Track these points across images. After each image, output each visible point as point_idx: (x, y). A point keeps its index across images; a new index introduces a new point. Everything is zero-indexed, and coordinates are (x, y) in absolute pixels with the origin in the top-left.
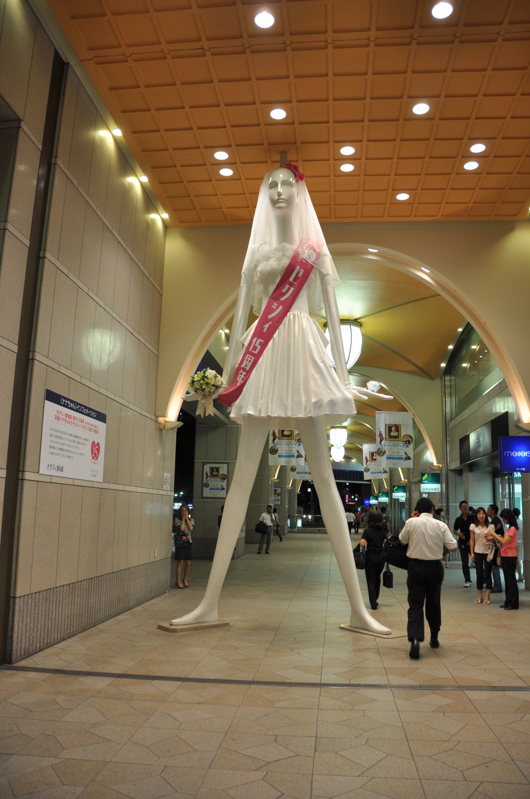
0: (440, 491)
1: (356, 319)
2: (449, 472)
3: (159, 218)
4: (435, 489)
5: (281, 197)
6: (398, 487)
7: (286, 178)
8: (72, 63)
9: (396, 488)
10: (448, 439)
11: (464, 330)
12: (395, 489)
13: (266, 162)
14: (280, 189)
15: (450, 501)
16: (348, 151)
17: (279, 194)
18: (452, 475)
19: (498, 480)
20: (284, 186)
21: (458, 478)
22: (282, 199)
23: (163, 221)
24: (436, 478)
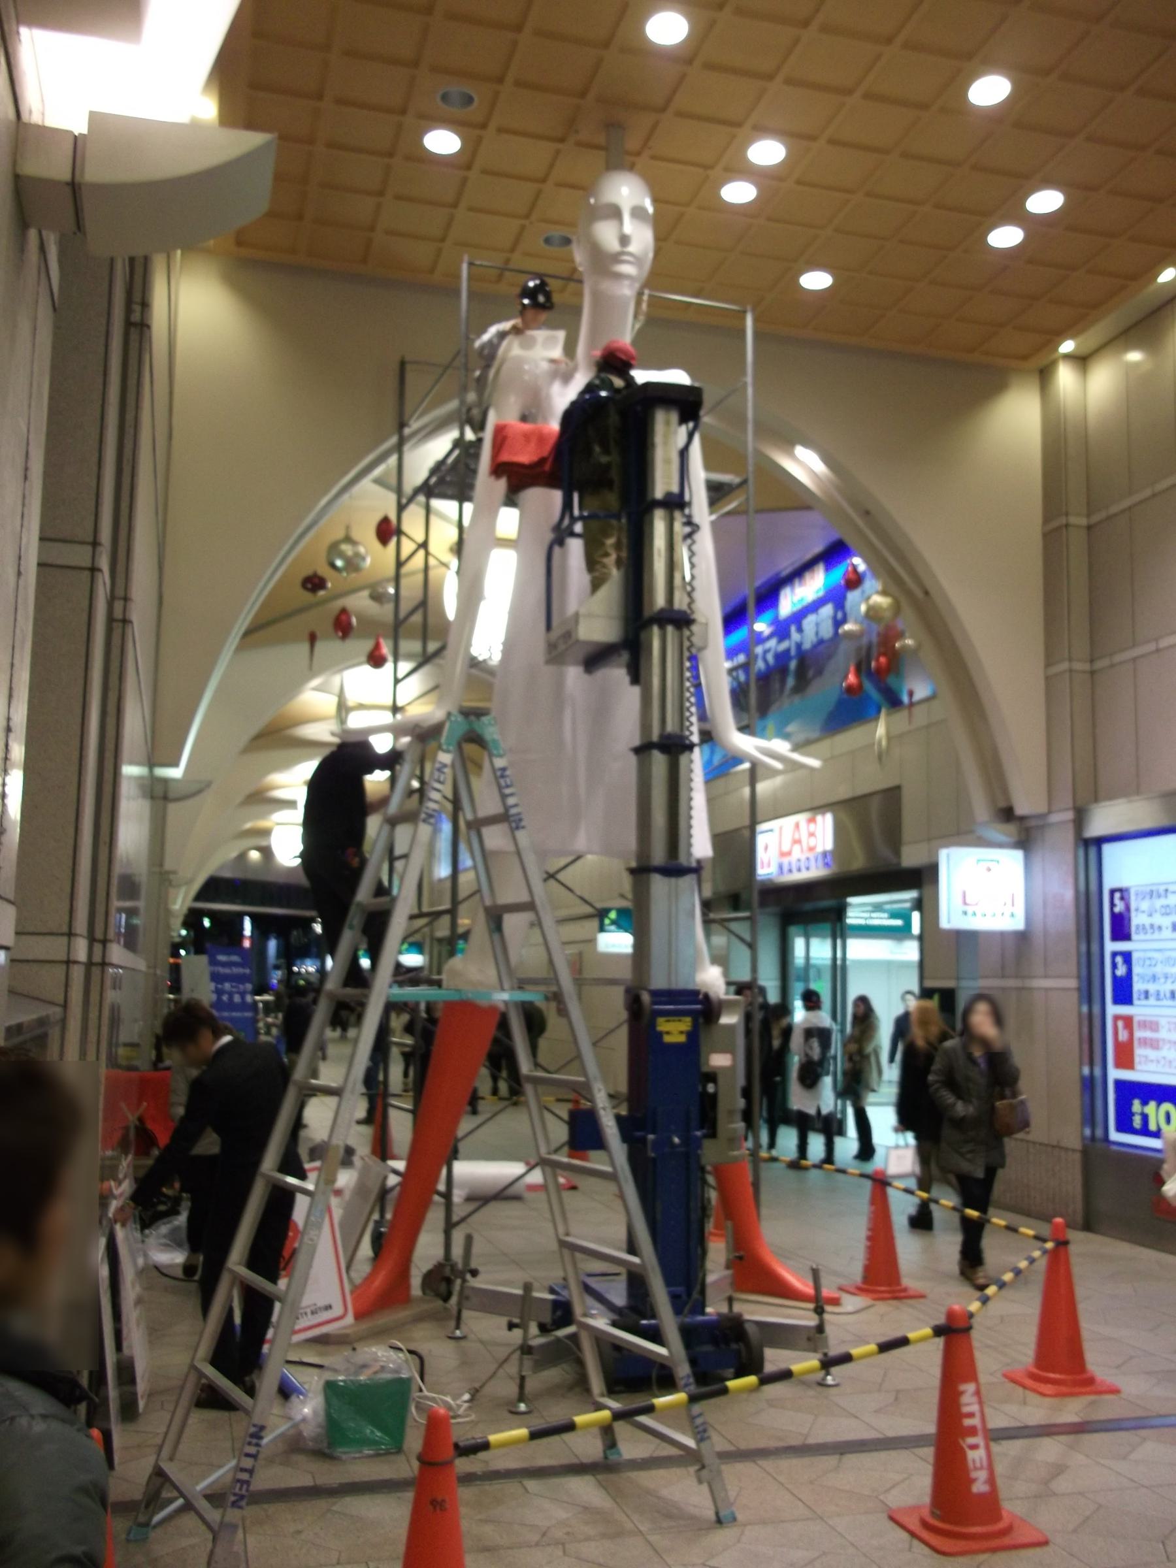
5: (632, 248)
7: (635, 201)
13: (562, 140)
16: (767, 152)
17: (624, 240)
19: (792, 930)
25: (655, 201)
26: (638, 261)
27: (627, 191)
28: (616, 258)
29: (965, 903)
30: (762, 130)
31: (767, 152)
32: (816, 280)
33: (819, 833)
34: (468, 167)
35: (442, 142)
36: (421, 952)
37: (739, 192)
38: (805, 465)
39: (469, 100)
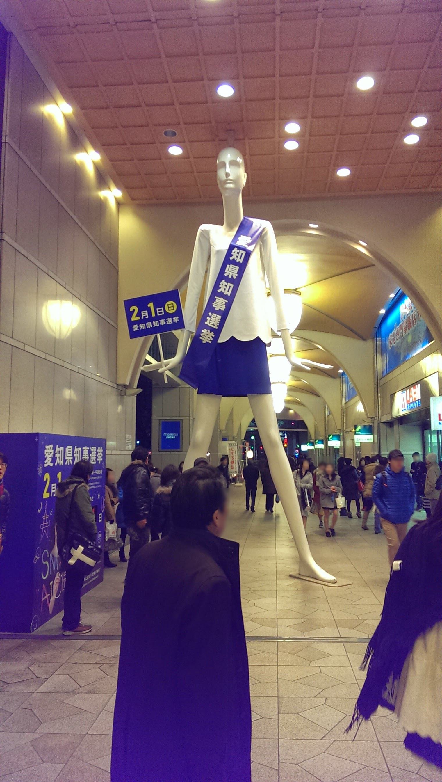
0: (372, 441)
1: (296, 289)
2: (381, 425)
3: (111, 195)
4: (368, 440)
5: (230, 178)
6: (333, 435)
7: (233, 159)
8: (14, 32)
9: (331, 436)
10: (379, 395)
11: (396, 296)
12: (330, 438)
14: (228, 170)
15: (382, 451)
16: (293, 128)
17: (227, 175)
18: (383, 427)
19: (427, 432)
20: (231, 167)
21: (389, 430)
22: (230, 180)
23: (116, 199)
24: (369, 430)
25: (244, 156)
26: (236, 181)
27: (228, 156)
28: (225, 182)
29: (440, 419)
30: (286, 120)
31: (293, 128)
32: (344, 173)
33: (417, 392)
34: (189, 158)
35: (175, 151)
36: (323, 443)
37: (291, 146)
38: (361, 248)
39: (175, 134)
